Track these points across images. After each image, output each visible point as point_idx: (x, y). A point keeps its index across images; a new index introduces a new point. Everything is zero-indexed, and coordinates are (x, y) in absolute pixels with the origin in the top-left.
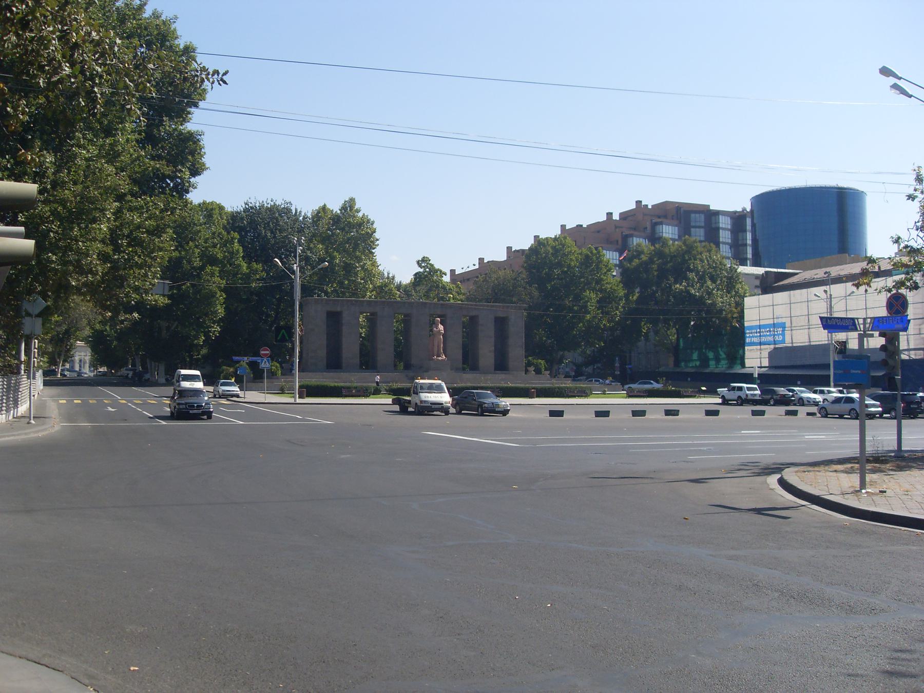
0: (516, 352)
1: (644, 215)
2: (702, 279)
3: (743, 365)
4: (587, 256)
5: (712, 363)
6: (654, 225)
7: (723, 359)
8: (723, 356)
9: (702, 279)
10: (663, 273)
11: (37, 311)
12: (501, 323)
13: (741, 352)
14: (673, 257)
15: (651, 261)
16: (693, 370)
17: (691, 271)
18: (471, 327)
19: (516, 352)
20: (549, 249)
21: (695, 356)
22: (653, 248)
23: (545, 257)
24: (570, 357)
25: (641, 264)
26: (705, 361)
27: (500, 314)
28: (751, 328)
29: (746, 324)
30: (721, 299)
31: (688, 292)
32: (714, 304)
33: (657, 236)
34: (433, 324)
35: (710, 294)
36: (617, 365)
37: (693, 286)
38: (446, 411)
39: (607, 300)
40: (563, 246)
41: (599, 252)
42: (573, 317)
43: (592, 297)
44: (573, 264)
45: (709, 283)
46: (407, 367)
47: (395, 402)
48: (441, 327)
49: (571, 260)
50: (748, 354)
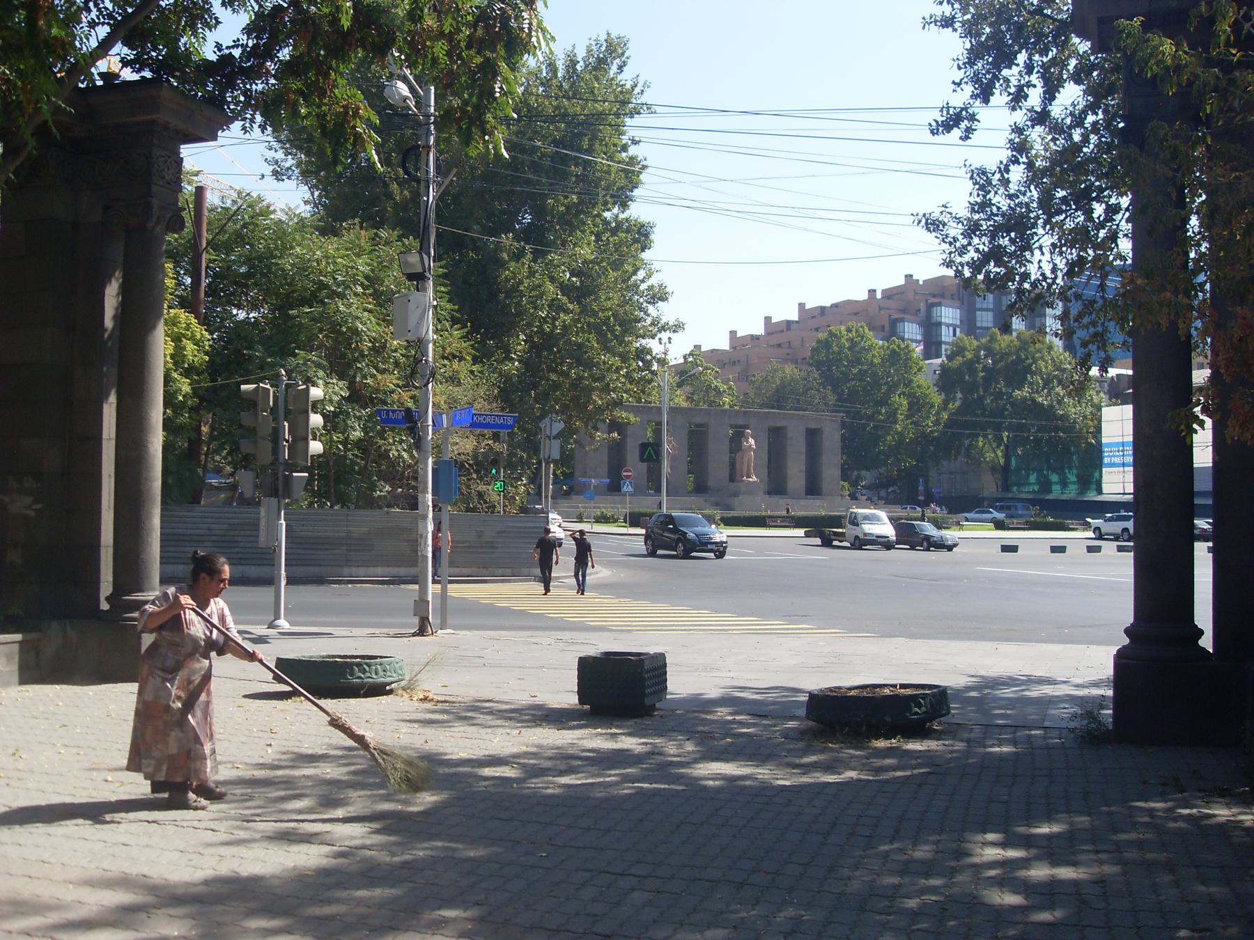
0: (831, 471)
1: (916, 293)
2: (1047, 382)
3: (1100, 491)
4: (893, 351)
5: (1056, 488)
6: (930, 307)
7: (1073, 483)
8: (1073, 479)
9: (1047, 382)
10: (991, 374)
11: (555, 433)
12: (813, 436)
13: (1096, 475)
14: (1004, 356)
15: (977, 359)
16: (1030, 497)
17: (1033, 373)
18: (776, 439)
19: (831, 471)
20: (843, 340)
21: (1033, 478)
22: (975, 343)
23: (839, 353)
24: (868, 477)
25: (964, 363)
26: (1046, 486)
27: (813, 425)
28: (1109, 445)
29: (1104, 441)
30: (1073, 409)
31: (1033, 400)
32: (1065, 417)
33: (933, 320)
34: (738, 436)
35: (1059, 402)
36: (921, 488)
37: (1038, 392)
38: (888, 546)
39: (917, 405)
40: (862, 337)
41: (907, 347)
42: (875, 427)
43: (901, 402)
44: (875, 360)
45: (1059, 389)
46: (700, 488)
47: (807, 535)
48: (752, 441)
49: (874, 356)
50: (1105, 478)
